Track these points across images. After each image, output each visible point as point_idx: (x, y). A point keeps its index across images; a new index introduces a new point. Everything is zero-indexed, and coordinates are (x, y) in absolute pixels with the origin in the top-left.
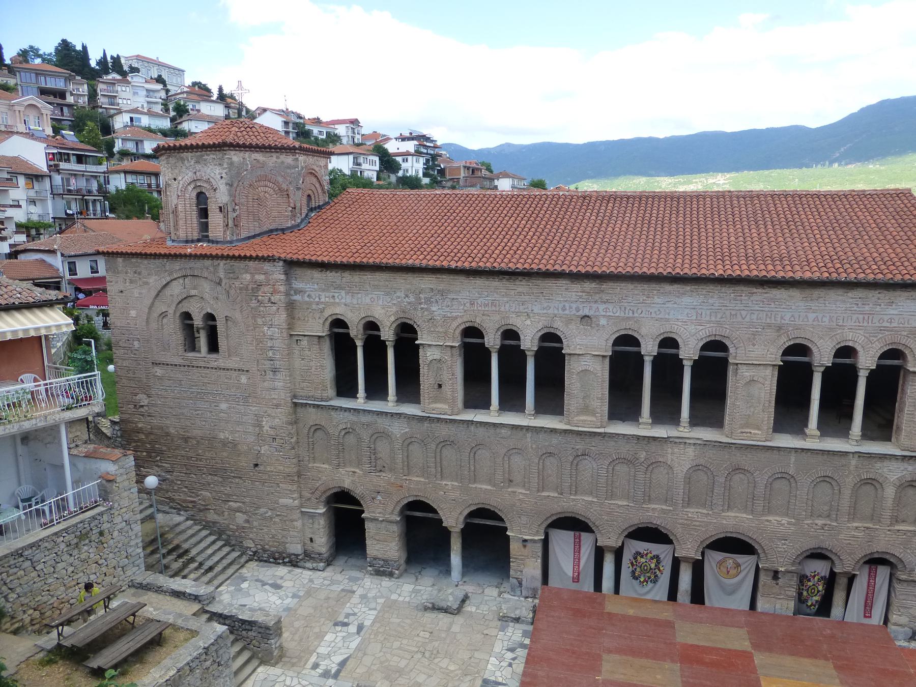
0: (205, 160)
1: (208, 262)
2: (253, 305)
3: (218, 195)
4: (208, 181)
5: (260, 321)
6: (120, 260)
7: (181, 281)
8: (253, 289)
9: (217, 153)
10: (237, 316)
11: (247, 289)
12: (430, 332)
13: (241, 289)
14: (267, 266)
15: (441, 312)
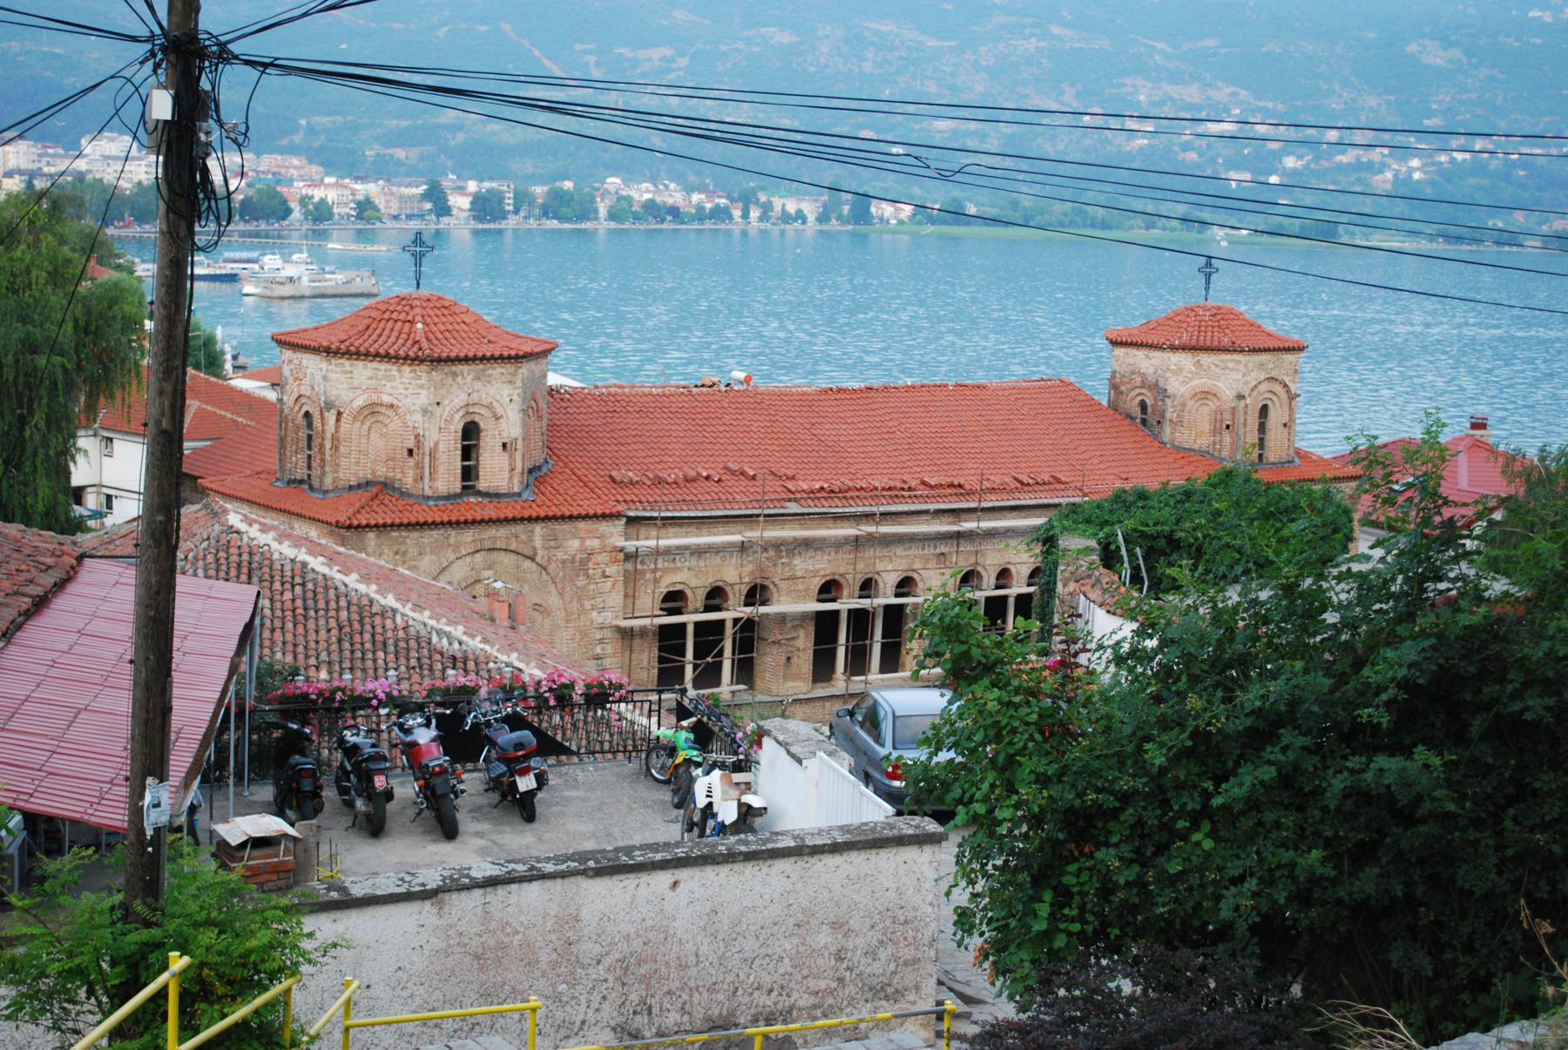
0: (490, 376)
1: (520, 528)
2: (579, 584)
3: (503, 424)
4: (489, 407)
5: (587, 605)
6: (371, 536)
7: (468, 559)
8: (581, 561)
9: (508, 366)
10: (554, 600)
11: (573, 558)
12: (790, 592)
13: (564, 562)
14: (604, 527)
15: (803, 565)
